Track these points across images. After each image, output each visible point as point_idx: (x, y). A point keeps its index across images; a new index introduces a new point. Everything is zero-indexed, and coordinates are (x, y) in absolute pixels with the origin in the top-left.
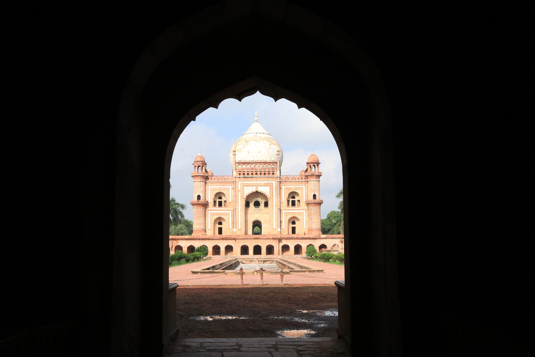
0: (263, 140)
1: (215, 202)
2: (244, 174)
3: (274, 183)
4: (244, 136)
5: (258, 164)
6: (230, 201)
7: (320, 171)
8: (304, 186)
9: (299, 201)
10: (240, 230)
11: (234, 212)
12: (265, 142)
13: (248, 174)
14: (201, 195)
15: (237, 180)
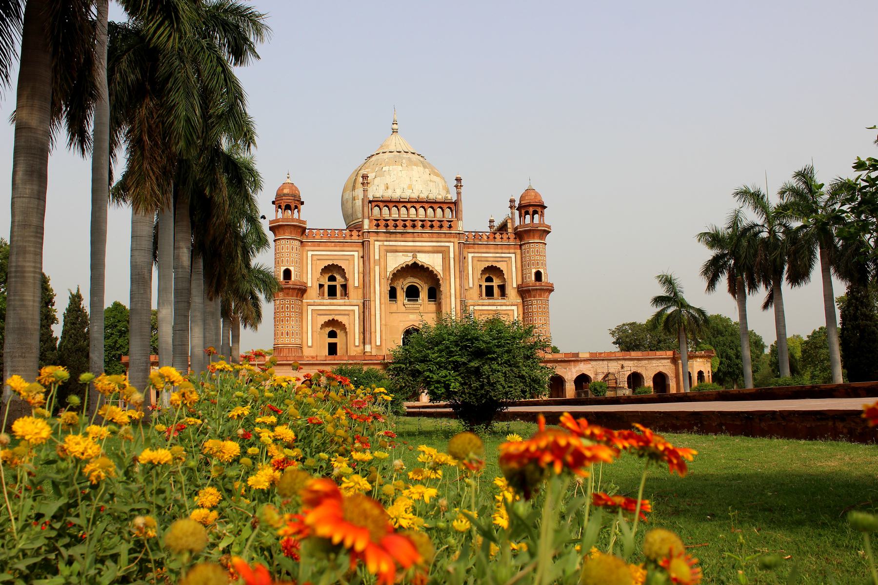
0: (416, 165)
1: (321, 286)
2: (387, 226)
3: (452, 247)
4: (373, 158)
5: (418, 206)
6: (356, 285)
7: (546, 222)
8: (513, 256)
9: (502, 288)
10: (379, 347)
11: (365, 306)
12: (421, 169)
13: (396, 226)
14: (292, 269)
15: (372, 239)
